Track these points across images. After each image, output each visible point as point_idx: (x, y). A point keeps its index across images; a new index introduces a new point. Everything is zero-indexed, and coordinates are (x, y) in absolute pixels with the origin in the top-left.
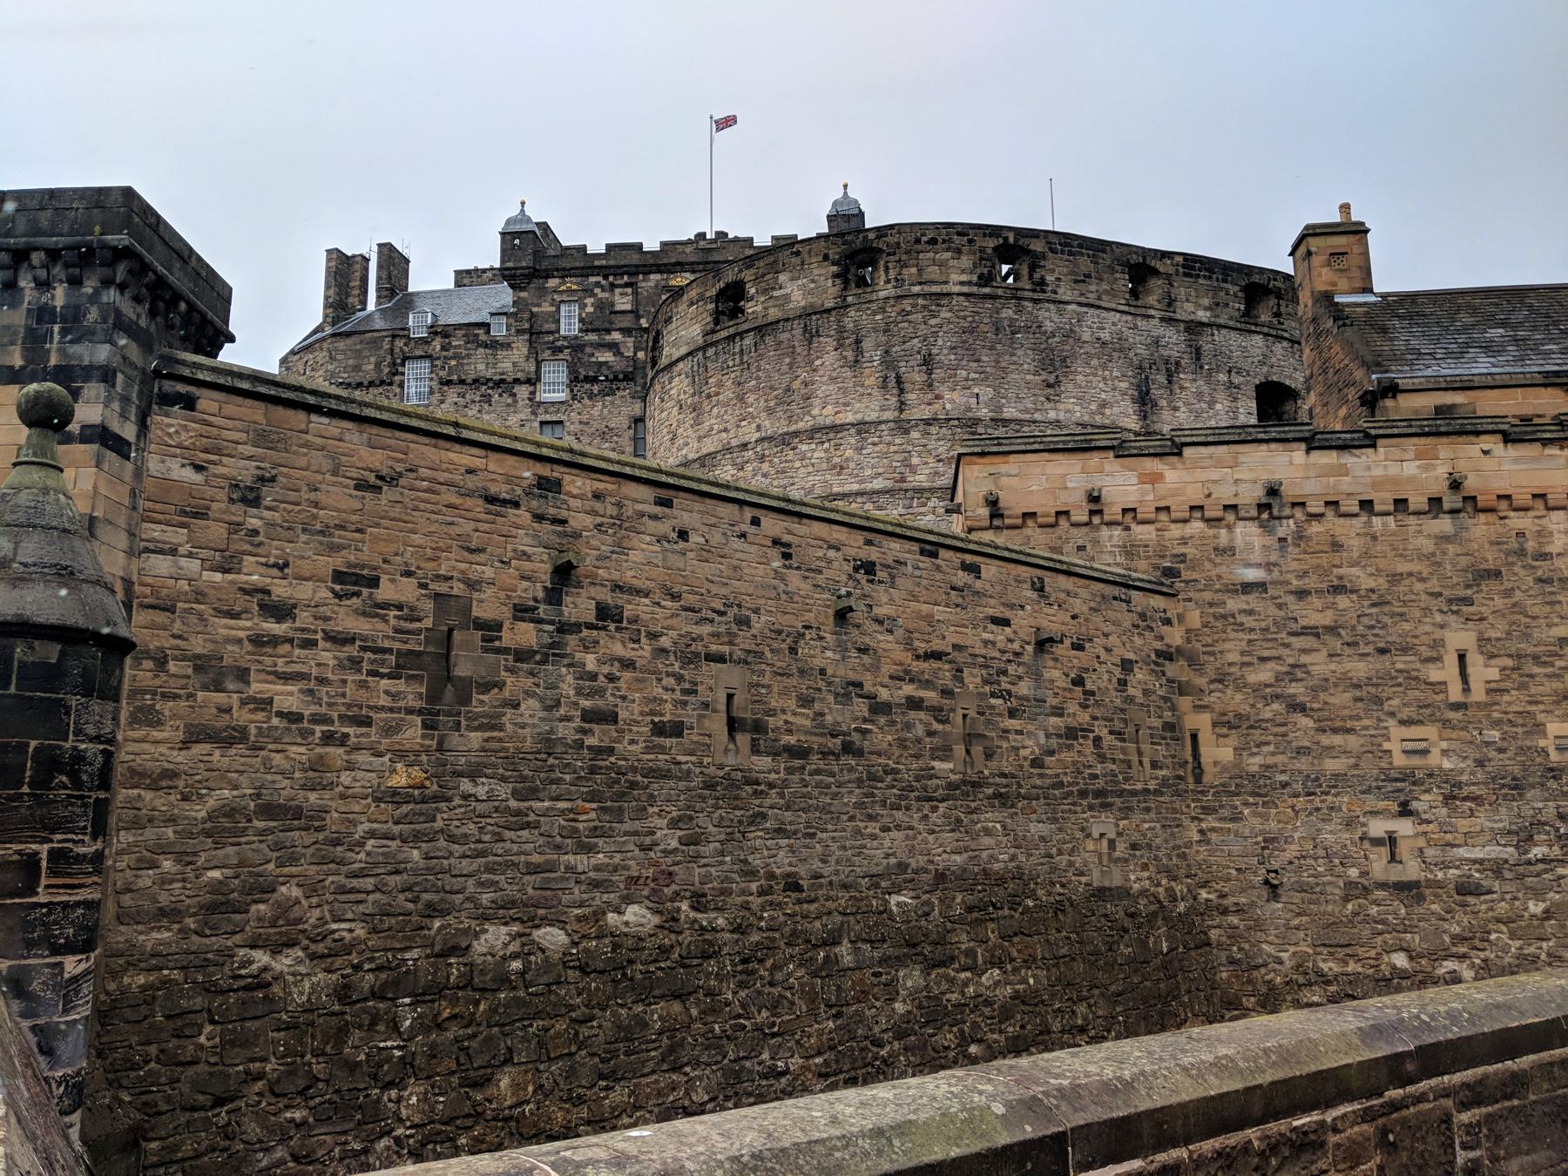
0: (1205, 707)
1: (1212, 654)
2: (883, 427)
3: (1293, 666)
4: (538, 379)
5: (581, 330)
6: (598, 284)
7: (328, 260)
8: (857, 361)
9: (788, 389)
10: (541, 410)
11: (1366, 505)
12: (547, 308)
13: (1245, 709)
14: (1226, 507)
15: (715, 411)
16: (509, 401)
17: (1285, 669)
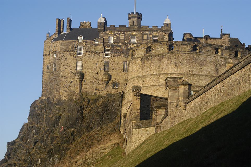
2: (174, 74)
4: (105, 52)
5: (113, 43)
6: (117, 33)
7: (56, 21)
8: (171, 63)
9: (159, 66)
10: (105, 58)
12: (106, 37)
15: (146, 68)
16: (99, 56)
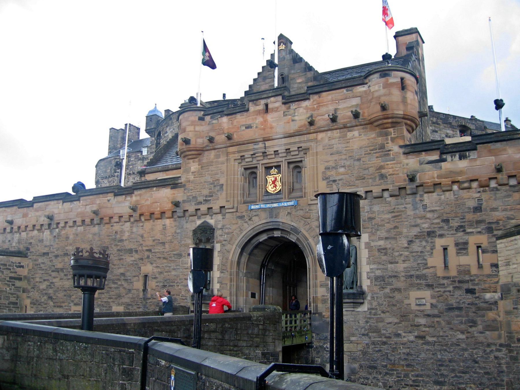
0: (29, 297)
1: (33, 278)
3: (51, 283)
11: (75, 222)
13: (38, 298)
14: (42, 225)
17: (48, 284)
